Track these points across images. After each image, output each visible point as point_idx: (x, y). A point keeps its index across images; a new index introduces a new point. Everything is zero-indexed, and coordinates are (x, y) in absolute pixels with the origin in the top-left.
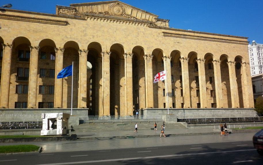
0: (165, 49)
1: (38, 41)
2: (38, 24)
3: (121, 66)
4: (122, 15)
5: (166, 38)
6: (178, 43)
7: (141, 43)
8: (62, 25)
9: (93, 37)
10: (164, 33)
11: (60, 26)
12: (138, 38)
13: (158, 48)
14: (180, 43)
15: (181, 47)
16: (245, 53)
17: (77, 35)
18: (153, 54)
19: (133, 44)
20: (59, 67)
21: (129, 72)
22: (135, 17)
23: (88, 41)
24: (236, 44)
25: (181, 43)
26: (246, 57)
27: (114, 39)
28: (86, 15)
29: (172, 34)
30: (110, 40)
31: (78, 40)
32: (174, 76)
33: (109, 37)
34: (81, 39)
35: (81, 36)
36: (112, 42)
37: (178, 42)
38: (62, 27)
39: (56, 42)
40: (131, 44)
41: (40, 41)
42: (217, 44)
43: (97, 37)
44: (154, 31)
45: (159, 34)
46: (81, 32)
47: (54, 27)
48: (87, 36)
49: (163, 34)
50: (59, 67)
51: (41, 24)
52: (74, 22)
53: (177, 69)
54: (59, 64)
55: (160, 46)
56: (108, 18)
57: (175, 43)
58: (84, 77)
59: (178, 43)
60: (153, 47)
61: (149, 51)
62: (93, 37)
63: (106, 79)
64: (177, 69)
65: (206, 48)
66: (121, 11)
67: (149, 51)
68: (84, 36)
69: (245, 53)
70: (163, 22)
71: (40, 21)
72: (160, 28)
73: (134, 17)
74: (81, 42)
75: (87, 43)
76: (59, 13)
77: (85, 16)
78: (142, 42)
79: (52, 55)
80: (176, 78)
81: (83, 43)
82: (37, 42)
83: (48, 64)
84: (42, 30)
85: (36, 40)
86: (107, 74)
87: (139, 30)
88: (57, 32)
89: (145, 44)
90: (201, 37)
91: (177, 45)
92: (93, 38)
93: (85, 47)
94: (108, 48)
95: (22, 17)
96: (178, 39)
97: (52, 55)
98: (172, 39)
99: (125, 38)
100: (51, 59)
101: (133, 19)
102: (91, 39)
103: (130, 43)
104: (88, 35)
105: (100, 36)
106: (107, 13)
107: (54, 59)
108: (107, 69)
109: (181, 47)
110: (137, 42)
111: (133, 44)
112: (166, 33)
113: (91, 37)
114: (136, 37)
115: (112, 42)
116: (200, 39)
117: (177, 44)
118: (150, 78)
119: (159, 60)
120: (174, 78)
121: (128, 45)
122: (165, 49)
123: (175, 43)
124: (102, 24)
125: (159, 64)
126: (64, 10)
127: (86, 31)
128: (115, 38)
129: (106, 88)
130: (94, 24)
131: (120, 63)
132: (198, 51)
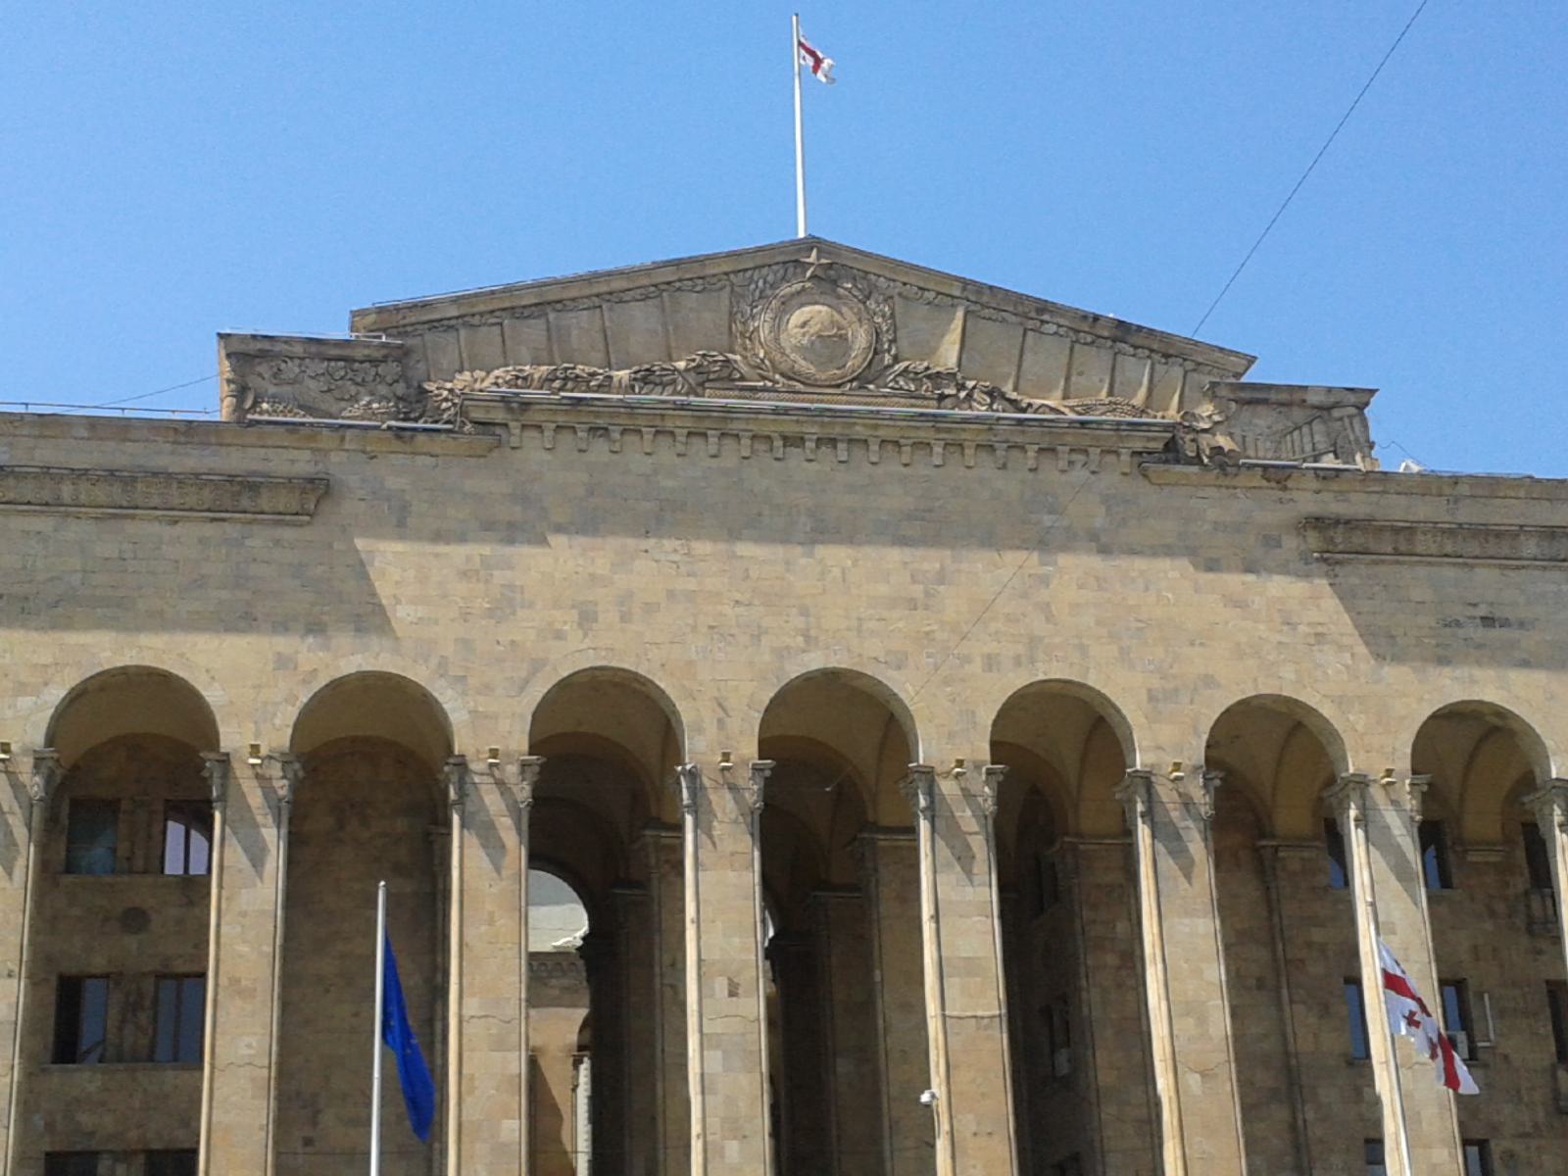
0: (1340, 701)
1: (36, 692)
2: (44, 524)
3: (887, 907)
4: (862, 379)
7: (1083, 649)
8: (280, 518)
9: (587, 618)
10: (1317, 523)
11: (259, 540)
12: (1044, 595)
13: (1267, 687)
14: (1505, 623)
17: (421, 611)
18: (1211, 762)
19: (991, 663)
20: (244, 949)
21: (971, 966)
23: (537, 666)
25: (1522, 625)
27: (799, 622)
28: (510, 410)
29: (1409, 530)
30: (757, 638)
31: (434, 662)
32: (1472, 984)
33: (740, 610)
34: (465, 644)
35: (465, 616)
36: (782, 653)
37: (1482, 611)
38: (277, 542)
39: (213, 695)
40: (976, 667)
41: (56, 694)
43: (625, 618)
44: (1212, 514)
45: (1271, 542)
46: (464, 575)
47: (203, 541)
48: (520, 613)
49: (1313, 539)
50: (244, 949)
51: (76, 530)
52: (393, 483)
53: (1501, 907)
54: (244, 914)
55: (1288, 673)
56: (721, 426)
57: (1458, 624)
58: (499, 1045)
59: (1488, 621)
60: (1209, 681)
61: (1167, 733)
62: (587, 618)
63: (724, 1052)
64: (1501, 907)
67: (1167, 733)
68: (490, 613)
70: (1298, 415)
71: (67, 491)
72: (1278, 476)
74: (462, 679)
75: (526, 682)
76: (248, 404)
77: (499, 416)
78: (1085, 641)
79: (175, 830)
80: (1501, 1013)
81: (487, 689)
82: (25, 702)
83: (135, 919)
84: (76, 579)
85: (21, 689)
86: (732, 994)
87: (1047, 520)
88: (224, 594)
89: (1124, 652)
91: (1479, 646)
92: (585, 635)
93: (504, 725)
94: (734, 724)
96: (1486, 583)
97: (175, 830)
99: (913, 605)
100: (173, 866)
101: (981, 410)
102: (559, 636)
103: (966, 659)
104: (531, 605)
105: (650, 608)
107: (197, 869)
108: (736, 940)
110: (1033, 641)
111: (991, 663)
112: (1349, 524)
113: (566, 620)
114: (1024, 596)
115: (782, 653)
117: (1479, 633)
118: (1202, 1020)
119: (1292, 817)
120: (1475, 1014)
121: (946, 682)
122: (1340, 701)
123: (1458, 624)
124: (670, 483)
125: (1292, 860)
126: (291, 369)
127: (512, 568)
128: (804, 612)
129: (733, 1148)
130: (591, 493)
131: (876, 870)
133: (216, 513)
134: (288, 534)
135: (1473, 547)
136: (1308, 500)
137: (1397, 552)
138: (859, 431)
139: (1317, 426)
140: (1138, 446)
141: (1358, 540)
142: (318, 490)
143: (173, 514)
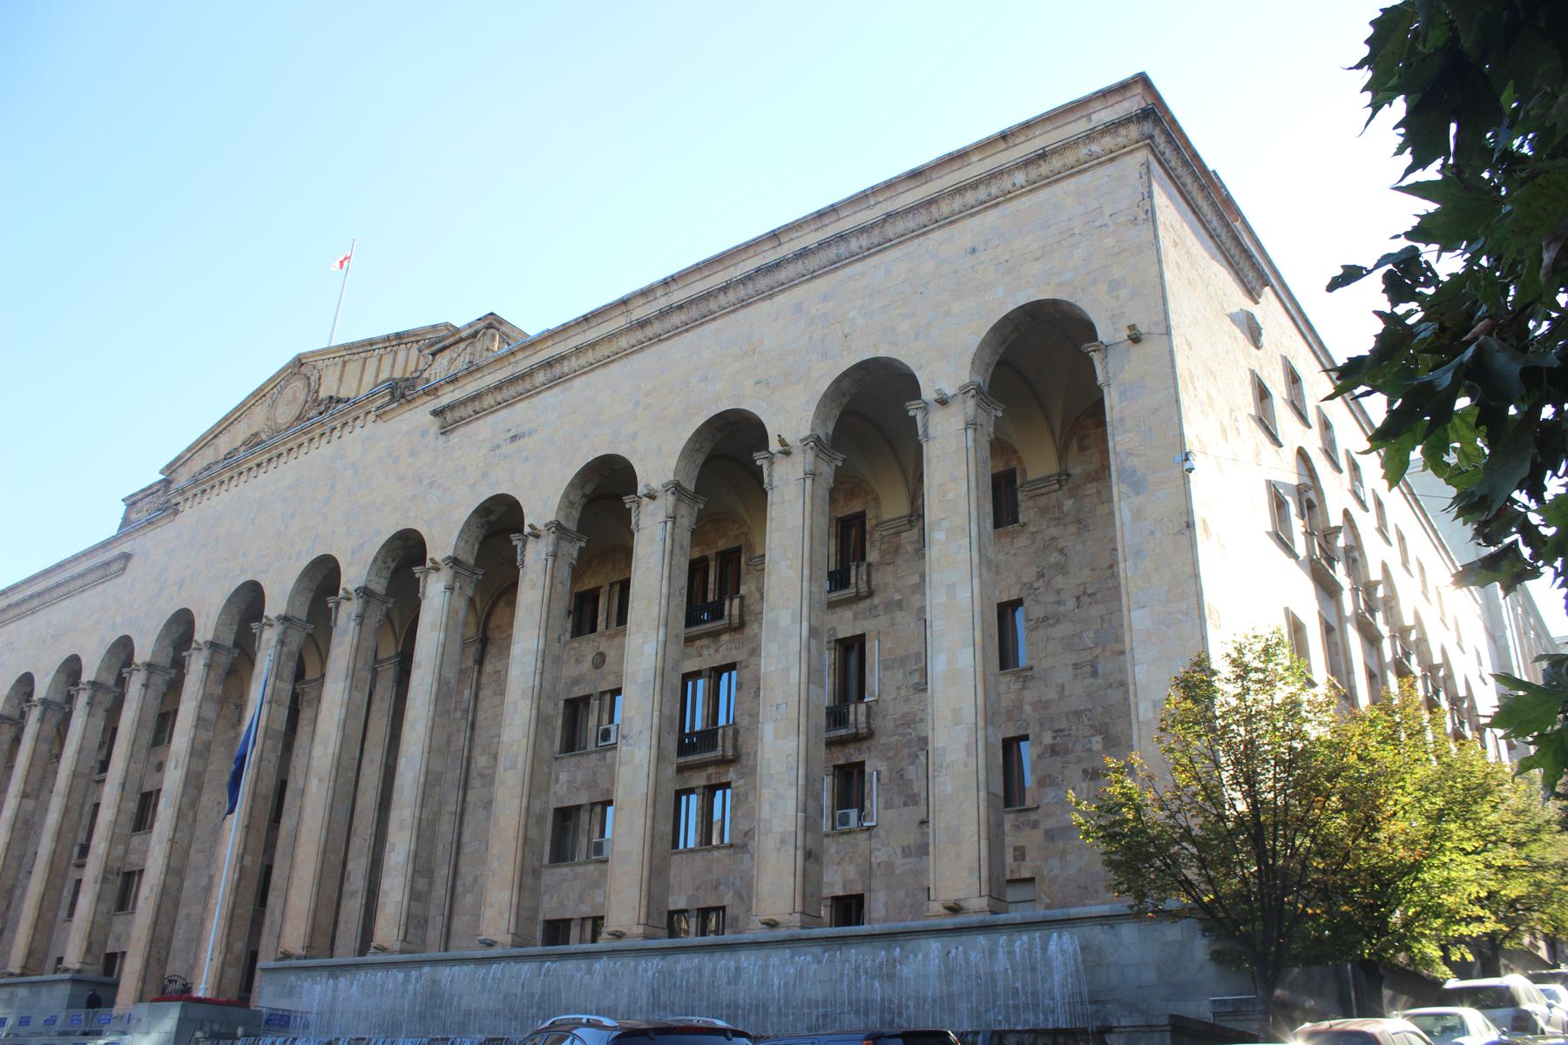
5: (455, 438)
6: (514, 438)
15: (526, 459)
16: (1110, 242)
22: (352, 395)
24: (992, 215)
25: (530, 433)
26: (1114, 286)
29: (478, 396)
42: (798, 307)
45: (425, 433)
59: (514, 438)
65: (702, 380)
66: (301, 397)
69: (1110, 242)
70: (462, 345)
72: (433, 391)
73: (339, 401)
90: (664, 314)
95: (40, 594)
96: (522, 413)
98: (486, 429)
106: (253, 442)
109: (526, 459)
112: (451, 407)
116: (658, 339)
123: (498, 447)
132: (635, 435)
133: (103, 579)
134: (119, 580)
135: (512, 391)
136: (446, 398)
137: (476, 412)
138: (283, 449)
139: (469, 350)
140: (379, 403)
141: (457, 414)
142: (127, 557)
143: (94, 584)
